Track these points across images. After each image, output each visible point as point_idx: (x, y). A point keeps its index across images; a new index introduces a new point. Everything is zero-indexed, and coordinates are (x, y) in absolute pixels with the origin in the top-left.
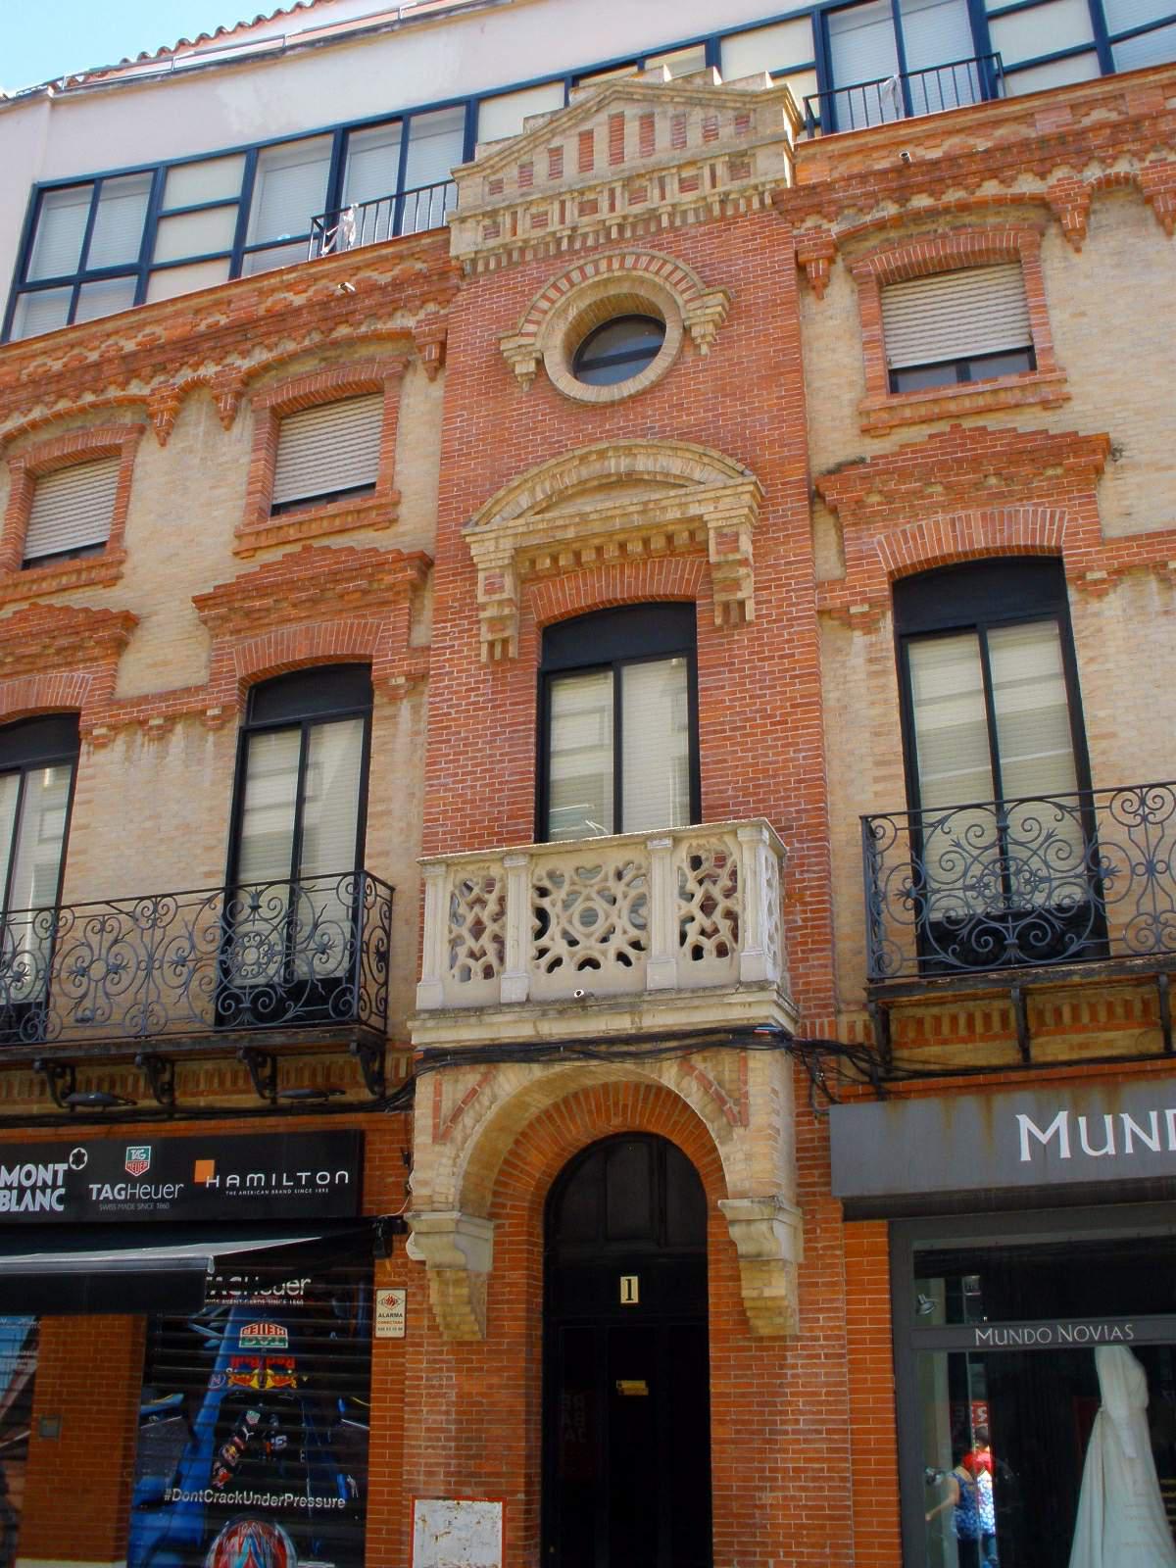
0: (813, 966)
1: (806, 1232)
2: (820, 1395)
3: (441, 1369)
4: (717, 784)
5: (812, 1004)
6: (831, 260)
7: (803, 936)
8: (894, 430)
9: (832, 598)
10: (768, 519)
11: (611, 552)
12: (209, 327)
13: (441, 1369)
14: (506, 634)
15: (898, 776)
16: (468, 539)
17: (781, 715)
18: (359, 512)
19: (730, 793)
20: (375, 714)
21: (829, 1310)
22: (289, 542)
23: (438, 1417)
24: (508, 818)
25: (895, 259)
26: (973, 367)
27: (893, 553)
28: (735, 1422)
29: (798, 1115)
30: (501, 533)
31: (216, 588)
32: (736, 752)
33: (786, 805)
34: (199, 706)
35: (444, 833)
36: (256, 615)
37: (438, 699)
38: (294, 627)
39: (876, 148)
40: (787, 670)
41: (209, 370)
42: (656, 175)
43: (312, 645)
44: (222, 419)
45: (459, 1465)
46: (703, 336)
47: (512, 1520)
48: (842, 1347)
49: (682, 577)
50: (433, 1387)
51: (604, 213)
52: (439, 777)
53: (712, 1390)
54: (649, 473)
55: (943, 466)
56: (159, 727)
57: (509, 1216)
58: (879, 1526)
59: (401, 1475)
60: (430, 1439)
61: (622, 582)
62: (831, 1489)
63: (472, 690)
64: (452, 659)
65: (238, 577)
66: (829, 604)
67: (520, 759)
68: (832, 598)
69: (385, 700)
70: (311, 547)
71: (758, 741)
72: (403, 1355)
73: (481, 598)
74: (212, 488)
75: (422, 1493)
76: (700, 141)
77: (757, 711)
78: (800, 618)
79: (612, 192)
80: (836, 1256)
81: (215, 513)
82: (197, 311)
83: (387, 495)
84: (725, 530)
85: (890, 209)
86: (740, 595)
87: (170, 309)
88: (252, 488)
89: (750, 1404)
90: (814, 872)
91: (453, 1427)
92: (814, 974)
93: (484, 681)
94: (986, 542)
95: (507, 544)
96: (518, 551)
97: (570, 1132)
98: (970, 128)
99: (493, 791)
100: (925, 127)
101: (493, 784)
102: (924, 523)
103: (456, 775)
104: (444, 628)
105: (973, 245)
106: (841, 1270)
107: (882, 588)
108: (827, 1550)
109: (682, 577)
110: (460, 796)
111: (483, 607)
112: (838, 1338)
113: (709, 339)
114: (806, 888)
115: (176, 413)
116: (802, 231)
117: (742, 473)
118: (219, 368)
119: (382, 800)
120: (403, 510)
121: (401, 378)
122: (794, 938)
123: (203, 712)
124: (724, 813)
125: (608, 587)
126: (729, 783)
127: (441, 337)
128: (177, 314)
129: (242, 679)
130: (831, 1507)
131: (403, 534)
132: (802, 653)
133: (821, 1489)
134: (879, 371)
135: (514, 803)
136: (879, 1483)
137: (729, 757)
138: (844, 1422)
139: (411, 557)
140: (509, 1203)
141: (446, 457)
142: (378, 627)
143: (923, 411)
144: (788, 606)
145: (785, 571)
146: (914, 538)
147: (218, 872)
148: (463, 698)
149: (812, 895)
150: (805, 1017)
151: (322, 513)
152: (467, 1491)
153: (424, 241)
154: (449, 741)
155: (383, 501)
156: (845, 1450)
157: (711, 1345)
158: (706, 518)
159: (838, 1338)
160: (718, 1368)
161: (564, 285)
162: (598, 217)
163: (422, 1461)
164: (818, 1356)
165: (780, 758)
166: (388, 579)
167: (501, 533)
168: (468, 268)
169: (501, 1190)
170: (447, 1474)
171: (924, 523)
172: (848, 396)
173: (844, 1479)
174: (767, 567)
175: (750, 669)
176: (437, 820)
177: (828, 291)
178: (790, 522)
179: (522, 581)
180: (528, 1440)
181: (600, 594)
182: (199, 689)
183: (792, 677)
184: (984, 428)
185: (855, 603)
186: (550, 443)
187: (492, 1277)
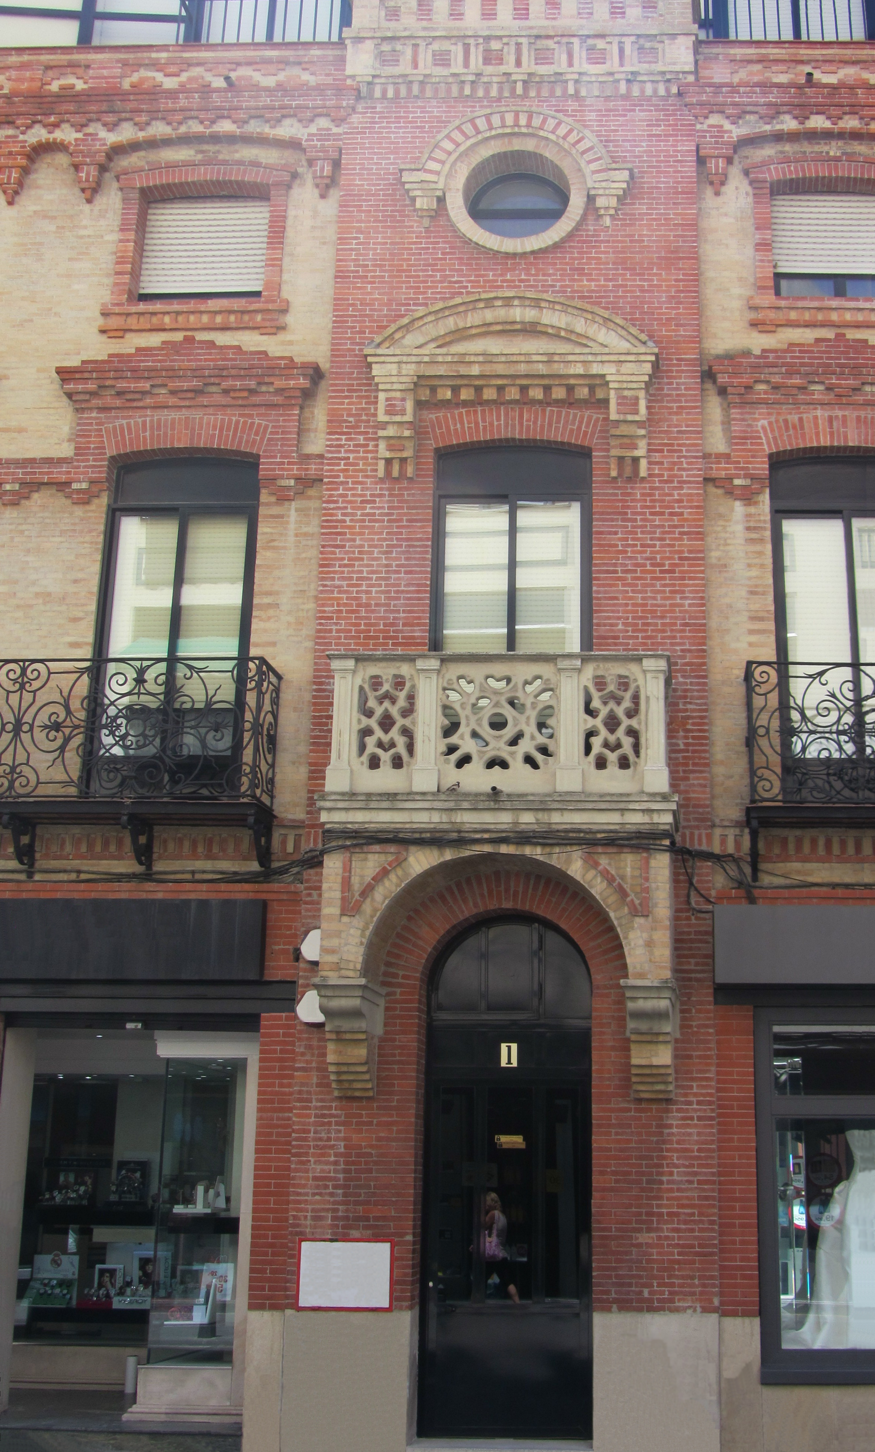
0: (693, 785)
1: (682, 1011)
2: (693, 1151)
3: (330, 1123)
4: (609, 618)
5: (691, 817)
6: (730, 161)
7: (684, 758)
8: (779, 329)
9: (717, 469)
10: (663, 389)
11: (513, 394)
12: (62, 88)
13: (330, 1123)
14: (405, 454)
15: (770, 631)
16: (369, 359)
17: (670, 565)
18: (243, 312)
19: (620, 627)
20: (262, 511)
21: (702, 1079)
22: (164, 330)
23: (326, 1167)
24: (404, 625)
25: (790, 172)
26: (849, 284)
27: (775, 438)
28: (614, 1173)
29: (677, 911)
30: (405, 359)
31: (83, 362)
32: (627, 592)
33: (672, 644)
34: (63, 478)
35: (338, 631)
36: (129, 397)
37: (332, 506)
38: (174, 415)
39: (777, 61)
40: (675, 527)
41: (67, 134)
42: (565, 40)
43: (193, 435)
44: (83, 190)
45: (347, 1211)
46: (607, 208)
47: (401, 1259)
48: (712, 1110)
49: (579, 428)
50: (321, 1139)
51: (509, 66)
52: (333, 579)
53: (594, 1145)
54: (553, 327)
55: (828, 371)
56: (13, 492)
57: (400, 985)
58: (741, 1261)
59: (287, 1220)
60: (317, 1187)
61: (521, 424)
62: (701, 1230)
63: (368, 502)
64: (347, 470)
65: (110, 356)
66: (714, 474)
67: (416, 572)
68: (717, 469)
69: (273, 499)
70: (193, 337)
71: (647, 585)
72: (290, 1110)
73: (382, 417)
74: (70, 259)
75: (309, 1236)
76: (607, 16)
77: (647, 559)
78: (689, 482)
79: (518, 45)
80: (709, 1034)
81: (76, 287)
82: (48, 68)
83: (274, 301)
84: (626, 393)
85: (789, 124)
86: (637, 453)
87: (14, 59)
88: (119, 268)
89: (629, 1158)
90: (696, 704)
91: (341, 1176)
92: (694, 792)
93: (380, 496)
94: (860, 442)
95: (410, 369)
96: (421, 381)
97: (462, 912)
98: (865, 62)
99: (389, 598)
100: (824, 52)
101: (389, 592)
102: (804, 416)
103: (351, 578)
104: (338, 439)
105: (863, 173)
106: (713, 1045)
107: (762, 467)
108: (696, 1281)
109: (579, 428)
110: (356, 599)
111: (384, 425)
112: (710, 1103)
113: (612, 212)
114: (689, 717)
115: (26, 171)
116: (705, 127)
117: (644, 343)
118: (80, 135)
119: (269, 594)
120: (289, 319)
121: (289, 187)
122: (677, 758)
123: (68, 484)
124: (616, 644)
125: (506, 426)
126: (619, 618)
127: (335, 155)
128: (23, 66)
129: (112, 457)
130: (700, 1246)
131: (291, 343)
132: (690, 513)
133: (692, 1230)
134: (769, 272)
135: (410, 612)
136: (742, 1226)
137: (620, 596)
138: (713, 1174)
139: (305, 366)
140: (401, 973)
141: (341, 275)
142: (266, 427)
143: (807, 316)
144: (679, 469)
145: (676, 439)
146: (794, 427)
147: (87, 644)
148: (359, 508)
149: (693, 724)
150: (684, 827)
151: (203, 308)
152: (355, 1233)
153: (312, 52)
154: (344, 546)
155: (270, 306)
156: (713, 1198)
157: (593, 1106)
158: (608, 378)
159: (710, 1103)
160: (600, 1126)
161: (468, 128)
162: (503, 69)
163: (310, 1207)
164: (692, 1118)
165: (668, 602)
166: (279, 383)
167: (405, 359)
168: (364, 90)
169: (393, 960)
170: (334, 1218)
171: (804, 416)
172: (737, 290)
173: (712, 1222)
174: (660, 432)
175: (642, 520)
176: (331, 618)
177: (724, 189)
178: (684, 395)
179: (419, 405)
180: (415, 1189)
181: (499, 432)
182: (61, 461)
183: (681, 533)
184: (866, 341)
185: (738, 477)
186: (450, 282)
187: (382, 1040)
